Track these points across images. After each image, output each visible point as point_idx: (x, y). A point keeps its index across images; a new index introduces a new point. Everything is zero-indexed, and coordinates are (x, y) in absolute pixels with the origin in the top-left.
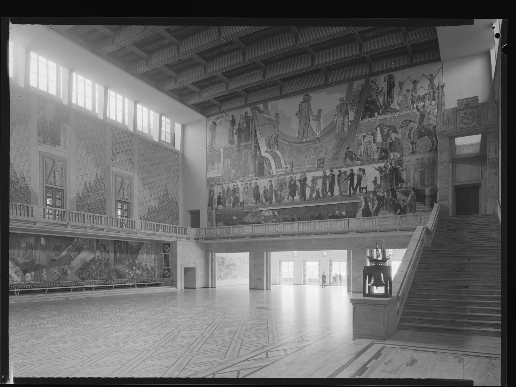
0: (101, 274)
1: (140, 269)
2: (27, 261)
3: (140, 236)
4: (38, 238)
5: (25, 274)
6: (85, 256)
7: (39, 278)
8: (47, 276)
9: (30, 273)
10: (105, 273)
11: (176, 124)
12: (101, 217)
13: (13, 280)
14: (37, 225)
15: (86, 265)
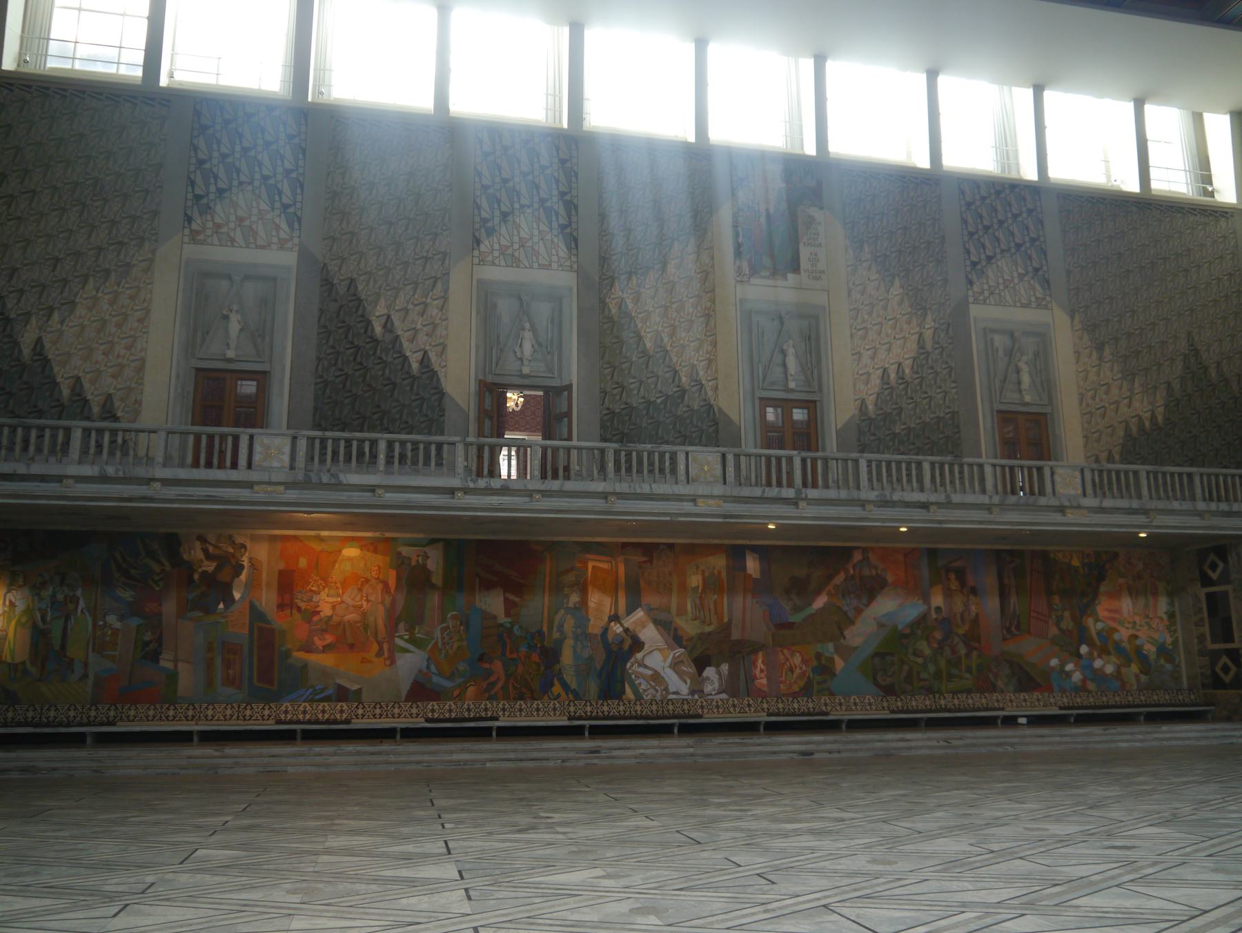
0: (955, 671)
1: (1109, 653)
2: (708, 629)
3: (1075, 521)
4: (737, 553)
5: (700, 670)
6: (892, 608)
7: (742, 685)
8: (768, 680)
9: (717, 666)
10: (969, 670)
11: (1208, 118)
12: (919, 464)
13: (666, 689)
14: (702, 507)
15: (896, 642)
